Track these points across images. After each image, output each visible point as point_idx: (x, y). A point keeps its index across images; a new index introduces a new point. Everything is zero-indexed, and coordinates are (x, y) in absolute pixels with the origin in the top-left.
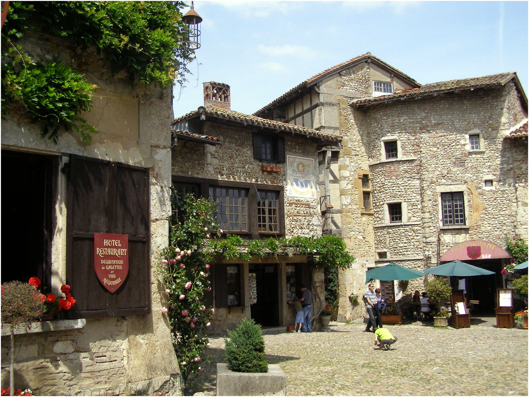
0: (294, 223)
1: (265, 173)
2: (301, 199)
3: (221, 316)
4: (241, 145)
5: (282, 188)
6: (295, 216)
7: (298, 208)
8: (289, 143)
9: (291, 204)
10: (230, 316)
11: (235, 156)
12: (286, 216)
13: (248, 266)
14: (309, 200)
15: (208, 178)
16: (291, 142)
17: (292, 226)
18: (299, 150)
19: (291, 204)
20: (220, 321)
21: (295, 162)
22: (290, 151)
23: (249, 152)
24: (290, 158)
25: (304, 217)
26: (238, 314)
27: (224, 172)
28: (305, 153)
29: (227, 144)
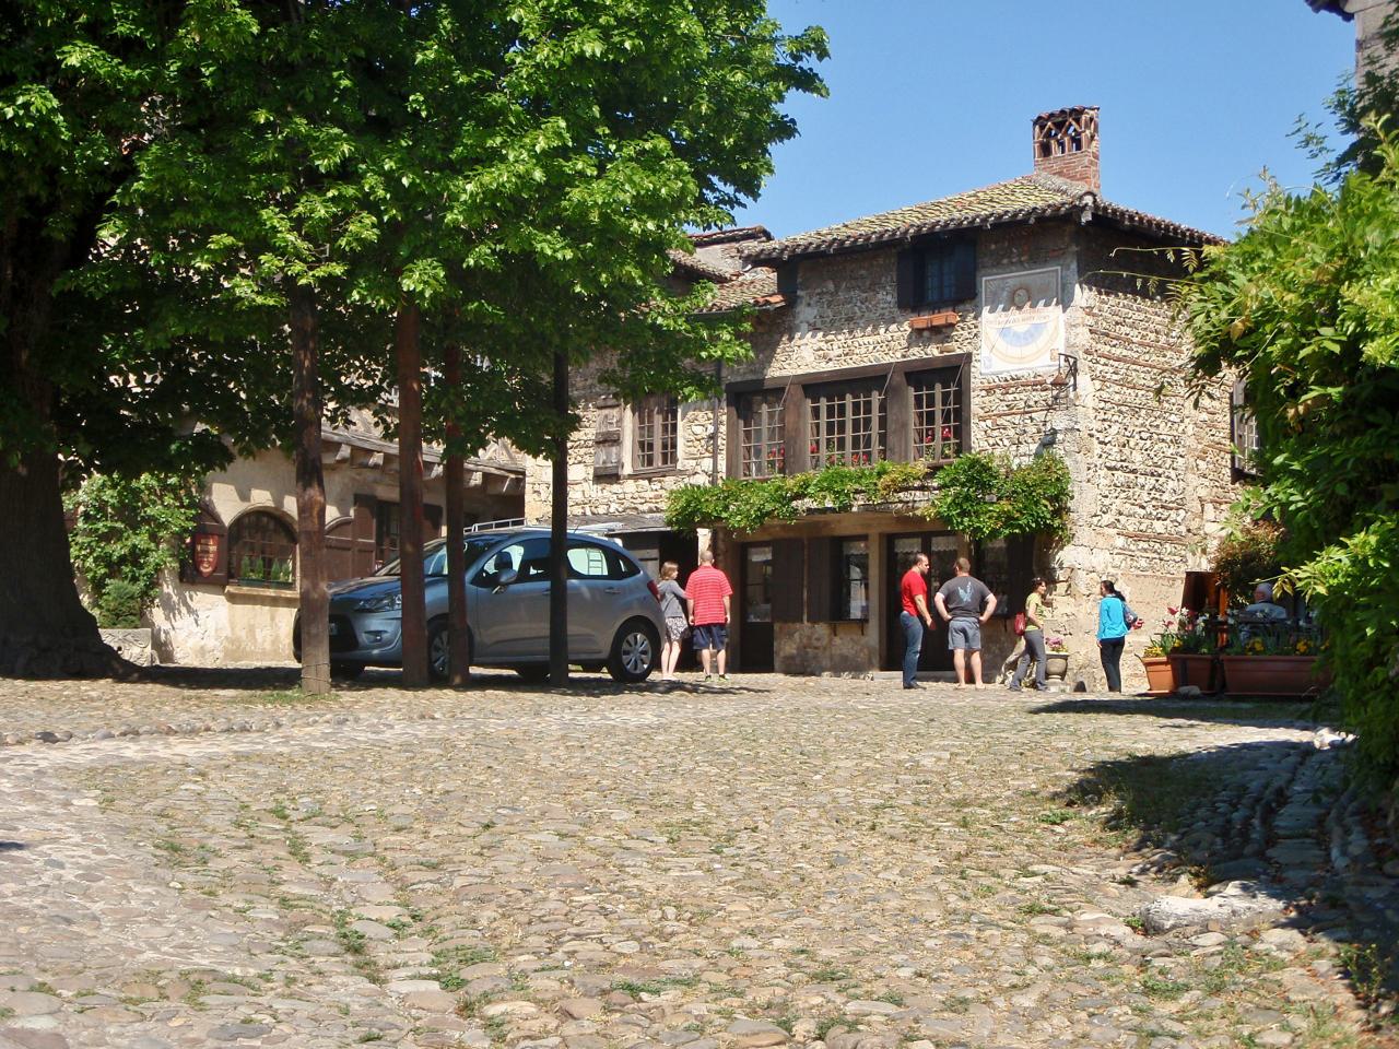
0: (996, 433)
1: (926, 334)
2: (1020, 374)
3: (818, 639)
4: (874, 287)
5: (969, 356)
6: (1000, 416)
7: (1010, 397)
8: (993, 247)
9: (989, 391)
10: (837, 640)
11: (859, 314)
12: (974, 420)
13: (877, 538)
14: (1040, 371)
15: (800, 372)
16: (995, 243)
17: (991, 441)
18: (1020, 255)
19: (989, 391)
20: (816, 648)
21: (1003, 289)
22: (993, 266)
23: (889, 298)
24: (987, 282)
25: (1027, 416)
26: (855, 637)
27: (832, 354)
28: (1037, 258)
29: (842, 296)
